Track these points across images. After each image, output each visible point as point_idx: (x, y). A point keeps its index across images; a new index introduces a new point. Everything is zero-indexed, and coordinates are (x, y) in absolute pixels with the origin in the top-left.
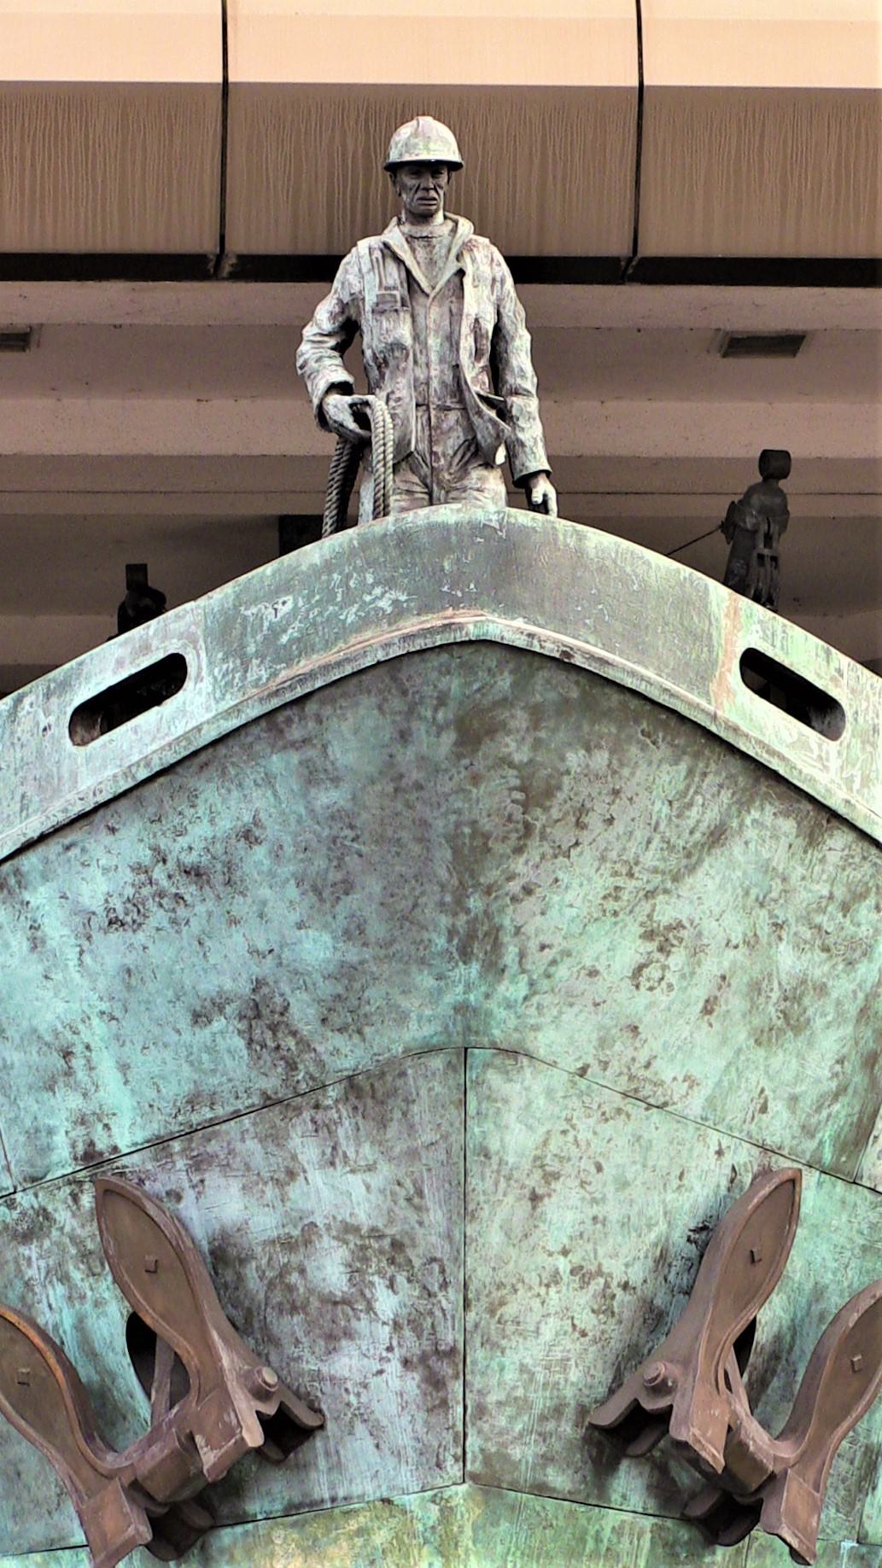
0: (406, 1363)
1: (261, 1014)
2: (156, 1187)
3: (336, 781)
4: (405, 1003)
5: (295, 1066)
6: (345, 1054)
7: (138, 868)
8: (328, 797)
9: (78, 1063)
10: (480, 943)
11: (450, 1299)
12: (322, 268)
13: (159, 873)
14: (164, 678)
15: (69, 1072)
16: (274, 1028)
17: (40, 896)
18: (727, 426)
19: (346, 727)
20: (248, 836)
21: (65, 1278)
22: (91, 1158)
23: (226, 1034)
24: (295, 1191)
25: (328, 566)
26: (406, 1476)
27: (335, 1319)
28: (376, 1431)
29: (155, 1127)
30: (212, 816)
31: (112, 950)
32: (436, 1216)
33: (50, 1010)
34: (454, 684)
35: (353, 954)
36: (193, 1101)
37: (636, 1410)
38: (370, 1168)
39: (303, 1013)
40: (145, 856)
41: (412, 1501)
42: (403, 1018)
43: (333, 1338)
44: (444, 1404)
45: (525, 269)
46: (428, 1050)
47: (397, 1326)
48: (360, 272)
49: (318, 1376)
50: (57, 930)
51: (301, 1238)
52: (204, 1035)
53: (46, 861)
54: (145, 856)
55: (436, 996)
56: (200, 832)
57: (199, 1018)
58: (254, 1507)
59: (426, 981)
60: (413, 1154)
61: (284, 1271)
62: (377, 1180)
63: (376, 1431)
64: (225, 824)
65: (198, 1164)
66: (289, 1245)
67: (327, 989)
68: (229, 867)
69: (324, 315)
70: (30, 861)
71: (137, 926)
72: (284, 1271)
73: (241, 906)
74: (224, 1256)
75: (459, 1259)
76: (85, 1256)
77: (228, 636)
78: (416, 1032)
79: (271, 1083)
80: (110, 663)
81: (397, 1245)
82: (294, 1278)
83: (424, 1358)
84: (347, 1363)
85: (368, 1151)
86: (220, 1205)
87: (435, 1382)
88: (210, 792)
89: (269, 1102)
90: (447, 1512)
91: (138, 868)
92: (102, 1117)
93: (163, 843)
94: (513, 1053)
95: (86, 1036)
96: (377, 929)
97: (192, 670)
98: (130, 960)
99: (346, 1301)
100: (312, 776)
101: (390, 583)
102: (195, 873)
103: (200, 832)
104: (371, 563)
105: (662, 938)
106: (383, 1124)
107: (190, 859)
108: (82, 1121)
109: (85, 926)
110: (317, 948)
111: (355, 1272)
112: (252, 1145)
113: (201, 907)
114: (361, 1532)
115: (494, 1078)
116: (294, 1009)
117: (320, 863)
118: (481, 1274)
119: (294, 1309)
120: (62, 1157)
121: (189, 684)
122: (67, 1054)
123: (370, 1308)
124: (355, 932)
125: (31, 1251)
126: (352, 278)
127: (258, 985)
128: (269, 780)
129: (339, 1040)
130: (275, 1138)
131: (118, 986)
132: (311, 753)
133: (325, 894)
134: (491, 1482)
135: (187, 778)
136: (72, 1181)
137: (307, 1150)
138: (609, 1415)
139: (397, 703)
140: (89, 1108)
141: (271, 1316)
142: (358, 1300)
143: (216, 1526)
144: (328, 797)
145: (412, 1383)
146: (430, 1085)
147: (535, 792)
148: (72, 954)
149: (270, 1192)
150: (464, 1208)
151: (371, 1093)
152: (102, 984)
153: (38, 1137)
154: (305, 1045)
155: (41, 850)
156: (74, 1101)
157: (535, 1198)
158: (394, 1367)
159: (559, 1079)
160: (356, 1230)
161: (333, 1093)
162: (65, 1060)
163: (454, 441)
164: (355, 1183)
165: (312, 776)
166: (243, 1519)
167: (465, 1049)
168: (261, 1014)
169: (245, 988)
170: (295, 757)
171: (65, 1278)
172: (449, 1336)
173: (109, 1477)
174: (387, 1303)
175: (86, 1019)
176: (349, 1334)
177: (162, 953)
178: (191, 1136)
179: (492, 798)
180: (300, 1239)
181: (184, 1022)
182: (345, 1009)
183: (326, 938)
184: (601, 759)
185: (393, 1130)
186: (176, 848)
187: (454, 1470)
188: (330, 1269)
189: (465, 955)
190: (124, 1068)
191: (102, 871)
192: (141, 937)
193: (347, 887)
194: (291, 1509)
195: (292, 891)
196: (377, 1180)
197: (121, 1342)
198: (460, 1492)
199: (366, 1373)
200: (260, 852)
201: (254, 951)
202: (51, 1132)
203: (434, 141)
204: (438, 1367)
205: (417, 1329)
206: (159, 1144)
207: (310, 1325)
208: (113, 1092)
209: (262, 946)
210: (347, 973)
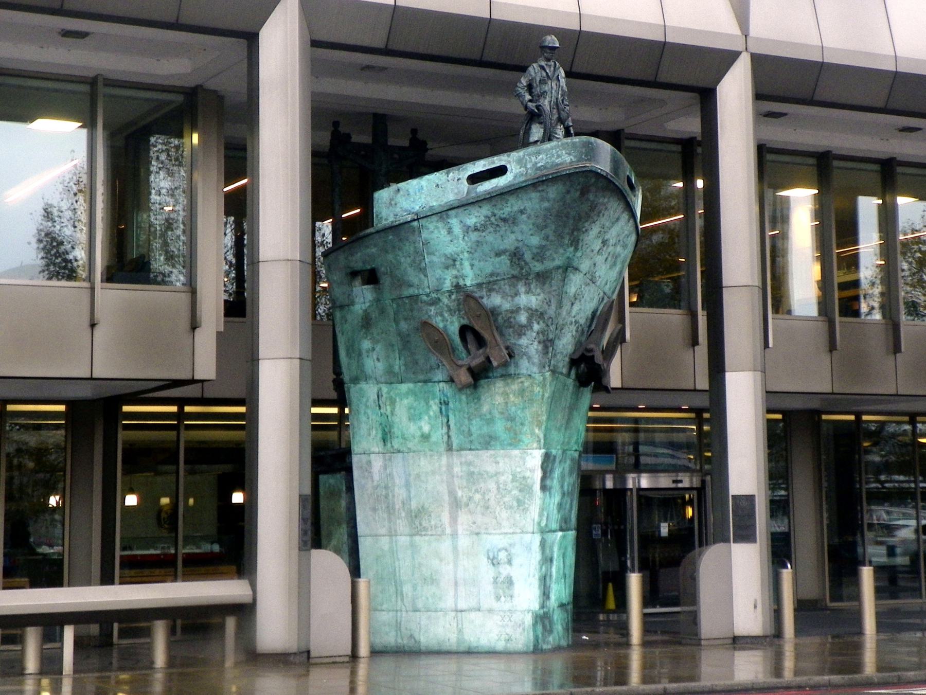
0: (539, 342)
1: (516, 256)
2: (477, 295)
3: (548, 201)
4: (555, 256)
5: (520, 269)
6: (538, 267)
7: (486, 217)
8: (546, 204)
9: (458, 263)
10: (575, 243)
11: (552, 328)
12: (523, 69)
13: (493, 219)
14: (501, 171)
15: (454, 265)
16: (519, 259)
17: (454, 222)
18: (613, 118)
19: (554, 188)
20: (522, 212)
21: (442, 315)
22: (457, 287)
23: (505, 259)
24: (517, 299)
25: (552, 148)
26: (535, 369)
27: (521, 330)
28: (529, 358)
29: (479, 281)
30: (512, 206)
31: (474, 236)
32: (553, 307)
33: (451, 249)
34: (582, 180)
35: (544, 243)
36: (492, 275)
37: (583, 356)
38: (539, 295)
39: (528, 256)
40: (490, 214)
41: (537, 376)
42: (554, 259)
43: (520, 335)
44: (547, 353)
45: (569, 75)
46: (558, 268)
47: (538, 333)
48: (534, 70)
49: (515, 344)
50: (457, 230)
51: (517, 310)
52: (498, 259)
53: (457, 213)
54: (490, 214)
55: (563, 254)
56: (507, 210)
57: (498, 254)
58: (491, 375)
59: (561, 251)
60: (549, 292)
61: (510, 318)
62: (539, 298)
63: (529, 358)
64: (516, 208)
65: (490, 290)
66: (512, 312)
67: (535, 251)
68: (515, 219)
69: (524, 81)
70: (453, 212)
71: (483, 231)
72: (510, 318)
73: (516, 229)
74: (493, 313)
75: (556, 317)
76: (450, 310)
77: (520, 162)
78: (557, 262)
79: (515, 272)
80: (481, 166)
81: (542, 314)
82: (512, 320)
83: (544, 341)
84: (524, 341)
85: (538, 290)
86: (495, 300)
87: (546, 347)
88: (512, 200)
89: (514, 277)
90: (544, 379)
91: (486, 217)
92: (463, 277)
93: (496, 212)
94: (576, 269)
95: (461, 256)
96: (551, 238)
97: (509, 170)
98: (479, 239)
99: (525, 326)
100: (542, 199)
101: (570, 154)
102: (504, 220)
103: (507, 210)
104: (565, 149)
105: (604, 242)
106: (544, 284)
107: (503, 216)
108: (456, 277)
109: (467, 230)
110: (535, 241)
111: (530, 320)
112: (507, 287)
113: (504, 227)
114: (522, 382)
115: (571, 275)
116: (526, 256)
117: (540, 221)
118: (561, 322)
119: (511, 327)
120: (447, 285)
121: (508, 173)
122: (454, 261)
123: (532, 328)
124: (547, 238)
125: (433, 308)
126: (533, 74)
127: (517, 248)
128: (530, 199)
129: (536, 264)
130: (514, 286)
131: (474, 246)
132: (544, 194)
133: (540, 228)
134: (554, 372)
135: (506, 197)
136: (451, 292)
137: (522, 288)
138: (576, 357)
139: (568, 183)
140: (458, 274)
141: (504, 329)
142: (529, 326)
143: (482, 378)
144: (546, 204)
145: (540, 347)
146: (558, 276)
147: (593, 208)
148: (461, 236)
149: (509, 298)
150: (560, 305)
151: (543, 277)
152: (469, 244)
153: (440, 280)
154: (526, 264)
155: (456, 210)
156: (455, 272)
157: (572, 304)
158: (536, 343)
159: (582, 275)
160: (531, 309)
161: (532, 276)
162: (452, 262)
163: (555, 117)
164: (533, 299)
165: (542, 199)
166: (488, 377)
167: (568, 268)
168: (516, 256)
169: (513, 248)
170: (538, 194)
171: (442, 315)
172: (551, 336)
173: (461, 366)
174: (536, 327)
175: (462, 252)
176: (524, 334)
177: (490, 238)
178: (490, 284)
179: (585, 207)
180: (517, 310)
181: (493, 255)
182: (540, 255)
183: (538, 238)
184: (606, 200)
185: (547, 285)
186: (499, 213)
187: (547, 368)
188: (523, 318)
189: (571, 245)
190: (472, 265)
191: (474, 218)
192: (484, 234)
193: (546, 227)
194: (502, 376)
195: (531, 226)
196: (539, 298)
197: (457, 332)
198: (548, 374)
199: (529, 344)
200: (524, 216)
201: (517, 240)
202: (445, 279)
203: (552, 41)
204: (547, 344)
205: (543, 335)
206: (479, 285)
207: (514, 332)
208: (467, 270)
209: (520, 238)
210: (542, 248)
